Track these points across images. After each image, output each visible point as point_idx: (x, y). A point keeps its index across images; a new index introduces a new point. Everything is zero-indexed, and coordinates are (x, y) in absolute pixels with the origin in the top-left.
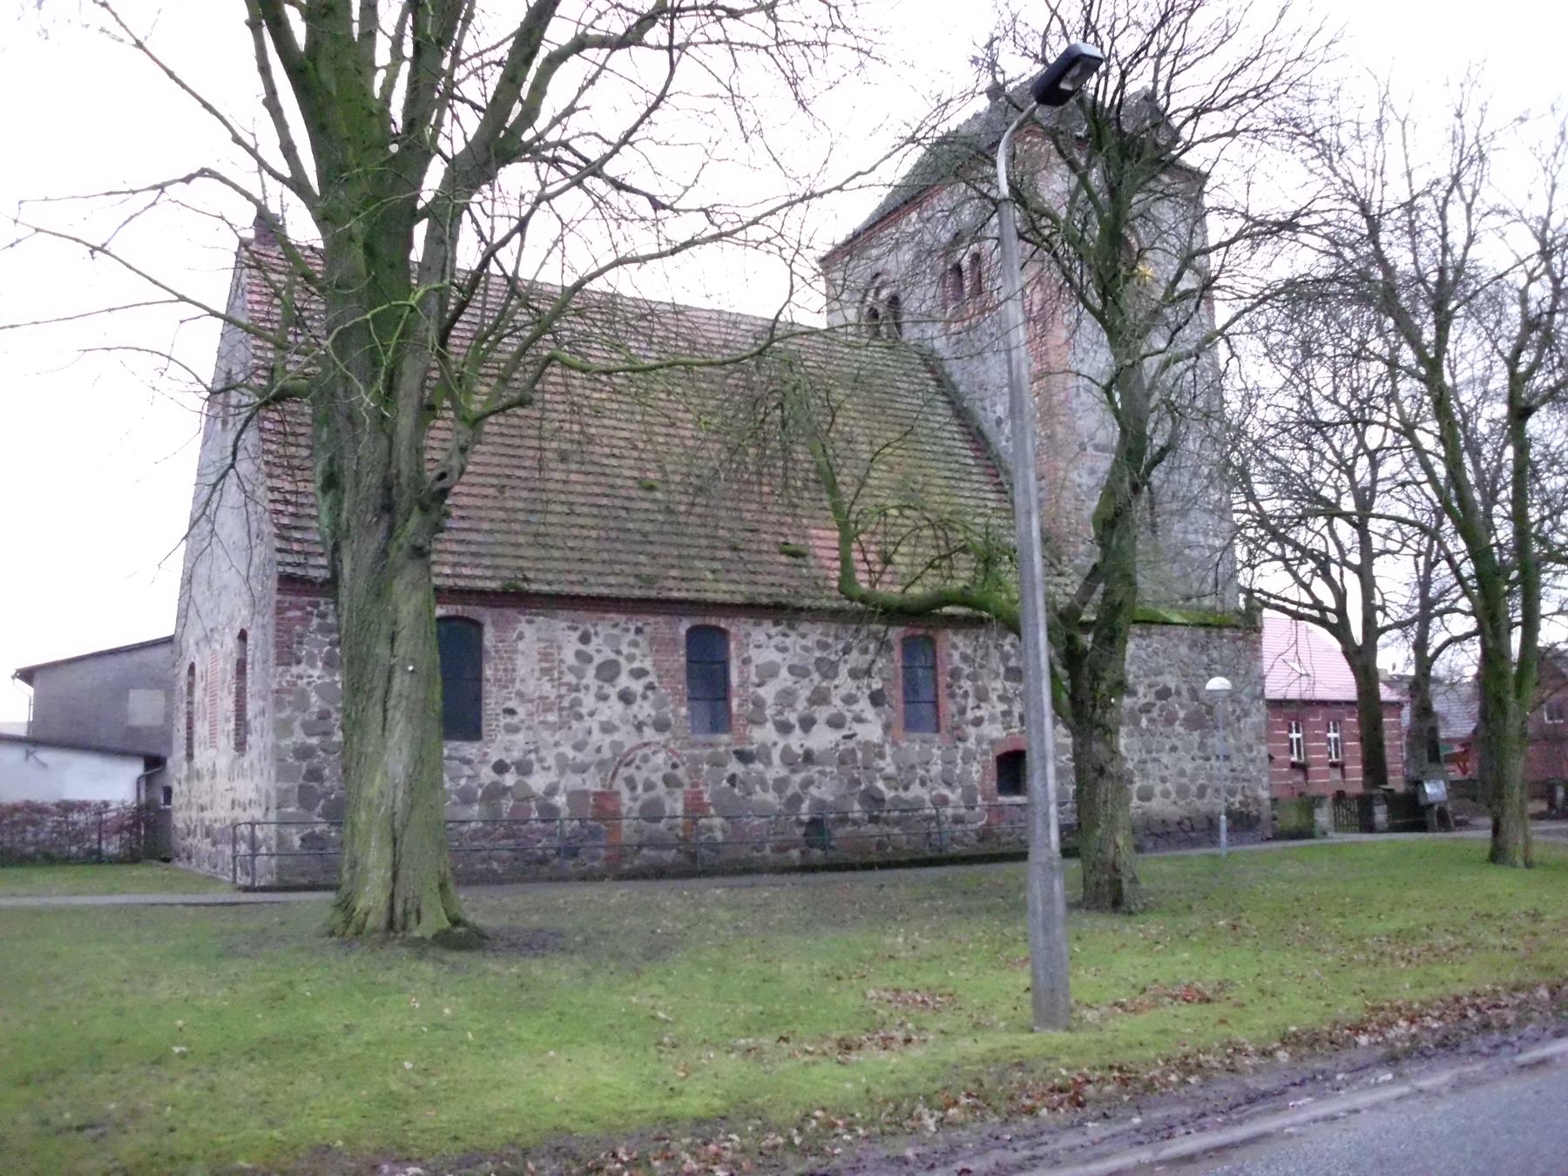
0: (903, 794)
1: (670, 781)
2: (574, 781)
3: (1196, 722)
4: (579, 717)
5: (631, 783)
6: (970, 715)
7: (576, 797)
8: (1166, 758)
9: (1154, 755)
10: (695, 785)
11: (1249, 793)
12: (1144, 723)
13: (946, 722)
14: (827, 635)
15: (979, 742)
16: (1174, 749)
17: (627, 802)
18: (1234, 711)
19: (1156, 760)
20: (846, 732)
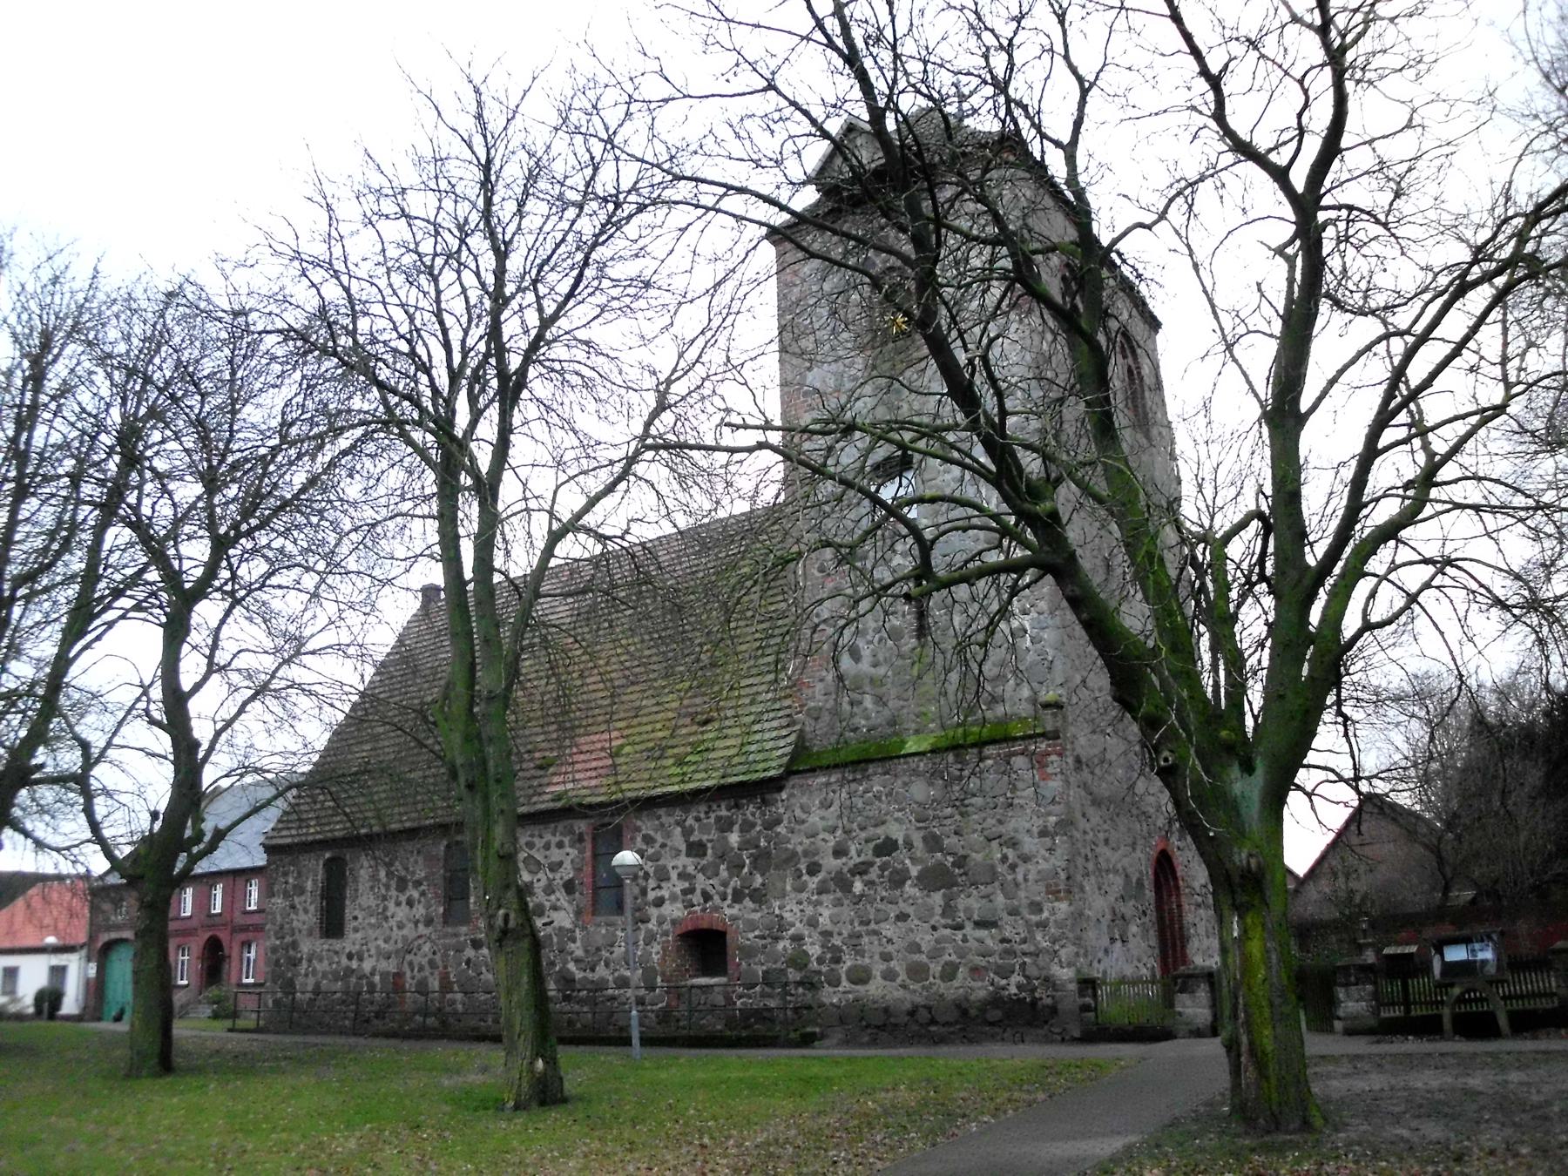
0: (590, 975)
1: (432, 964)
2: (384, 965)
3: (935, 879)
4: (386, 918)
5: (411, 964)
6: (651, 895)
7: (384, 975)
8: (888, 929)
9: (873, 926)
10: (445, 967)
11: (1032, 971)
12: (858, 887)
13: (628, 902)
14: (532, 836)
15: (660, 923)
16: (902, 917)
17: (409, 983)
18: (1004, 858)
19: (876, 933)
20: (546, 920)
